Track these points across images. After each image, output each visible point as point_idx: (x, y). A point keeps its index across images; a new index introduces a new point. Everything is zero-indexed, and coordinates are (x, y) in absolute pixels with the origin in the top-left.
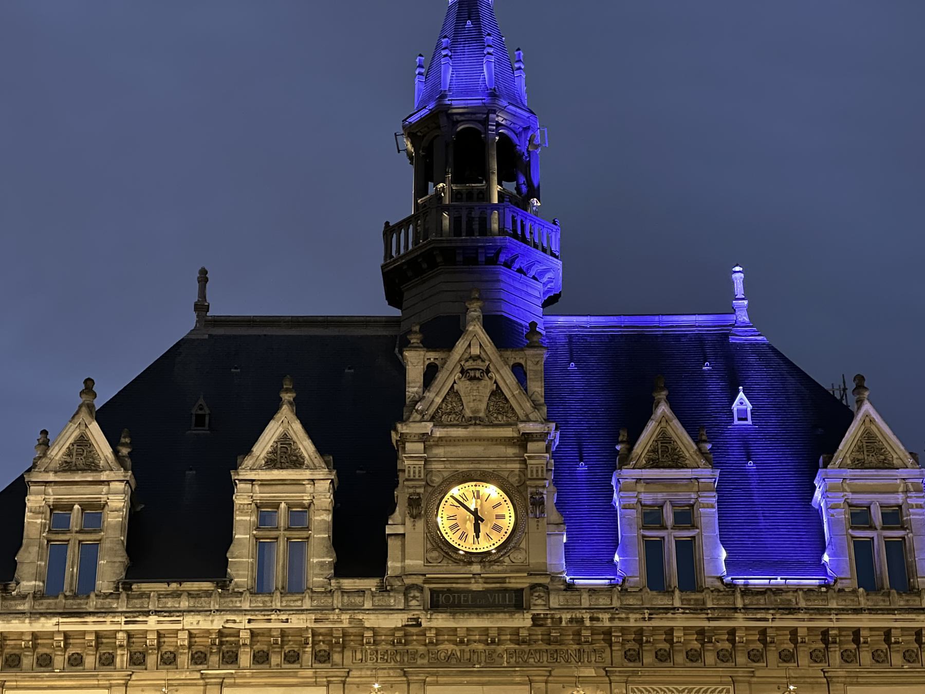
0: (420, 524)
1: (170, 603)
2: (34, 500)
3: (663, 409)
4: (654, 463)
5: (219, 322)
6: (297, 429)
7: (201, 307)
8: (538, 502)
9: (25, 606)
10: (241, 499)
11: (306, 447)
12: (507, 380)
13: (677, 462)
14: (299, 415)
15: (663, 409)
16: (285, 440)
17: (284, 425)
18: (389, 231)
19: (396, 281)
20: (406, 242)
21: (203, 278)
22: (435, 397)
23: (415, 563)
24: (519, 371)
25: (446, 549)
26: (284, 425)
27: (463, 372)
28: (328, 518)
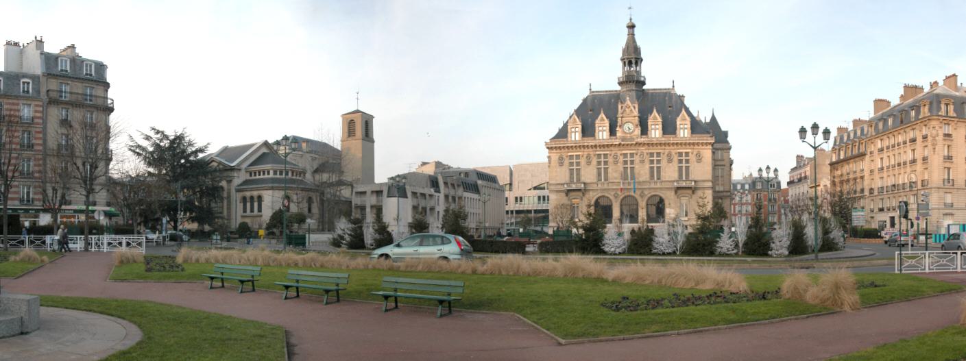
2: (569, 127)
3: (655, 111)
5: (593, 92)
6: (604, 116)
7: (590, 90)
10: (597, 125)
11: (605, 118)
12: (632, 108)
14: (604, 114)
15: (655, 111)
17: (602, 115)
18: (618, 78)
19: (620, 83)
21: (590, 85)
24: (634, 107)
25: (625, 133)
26: (602, 115)
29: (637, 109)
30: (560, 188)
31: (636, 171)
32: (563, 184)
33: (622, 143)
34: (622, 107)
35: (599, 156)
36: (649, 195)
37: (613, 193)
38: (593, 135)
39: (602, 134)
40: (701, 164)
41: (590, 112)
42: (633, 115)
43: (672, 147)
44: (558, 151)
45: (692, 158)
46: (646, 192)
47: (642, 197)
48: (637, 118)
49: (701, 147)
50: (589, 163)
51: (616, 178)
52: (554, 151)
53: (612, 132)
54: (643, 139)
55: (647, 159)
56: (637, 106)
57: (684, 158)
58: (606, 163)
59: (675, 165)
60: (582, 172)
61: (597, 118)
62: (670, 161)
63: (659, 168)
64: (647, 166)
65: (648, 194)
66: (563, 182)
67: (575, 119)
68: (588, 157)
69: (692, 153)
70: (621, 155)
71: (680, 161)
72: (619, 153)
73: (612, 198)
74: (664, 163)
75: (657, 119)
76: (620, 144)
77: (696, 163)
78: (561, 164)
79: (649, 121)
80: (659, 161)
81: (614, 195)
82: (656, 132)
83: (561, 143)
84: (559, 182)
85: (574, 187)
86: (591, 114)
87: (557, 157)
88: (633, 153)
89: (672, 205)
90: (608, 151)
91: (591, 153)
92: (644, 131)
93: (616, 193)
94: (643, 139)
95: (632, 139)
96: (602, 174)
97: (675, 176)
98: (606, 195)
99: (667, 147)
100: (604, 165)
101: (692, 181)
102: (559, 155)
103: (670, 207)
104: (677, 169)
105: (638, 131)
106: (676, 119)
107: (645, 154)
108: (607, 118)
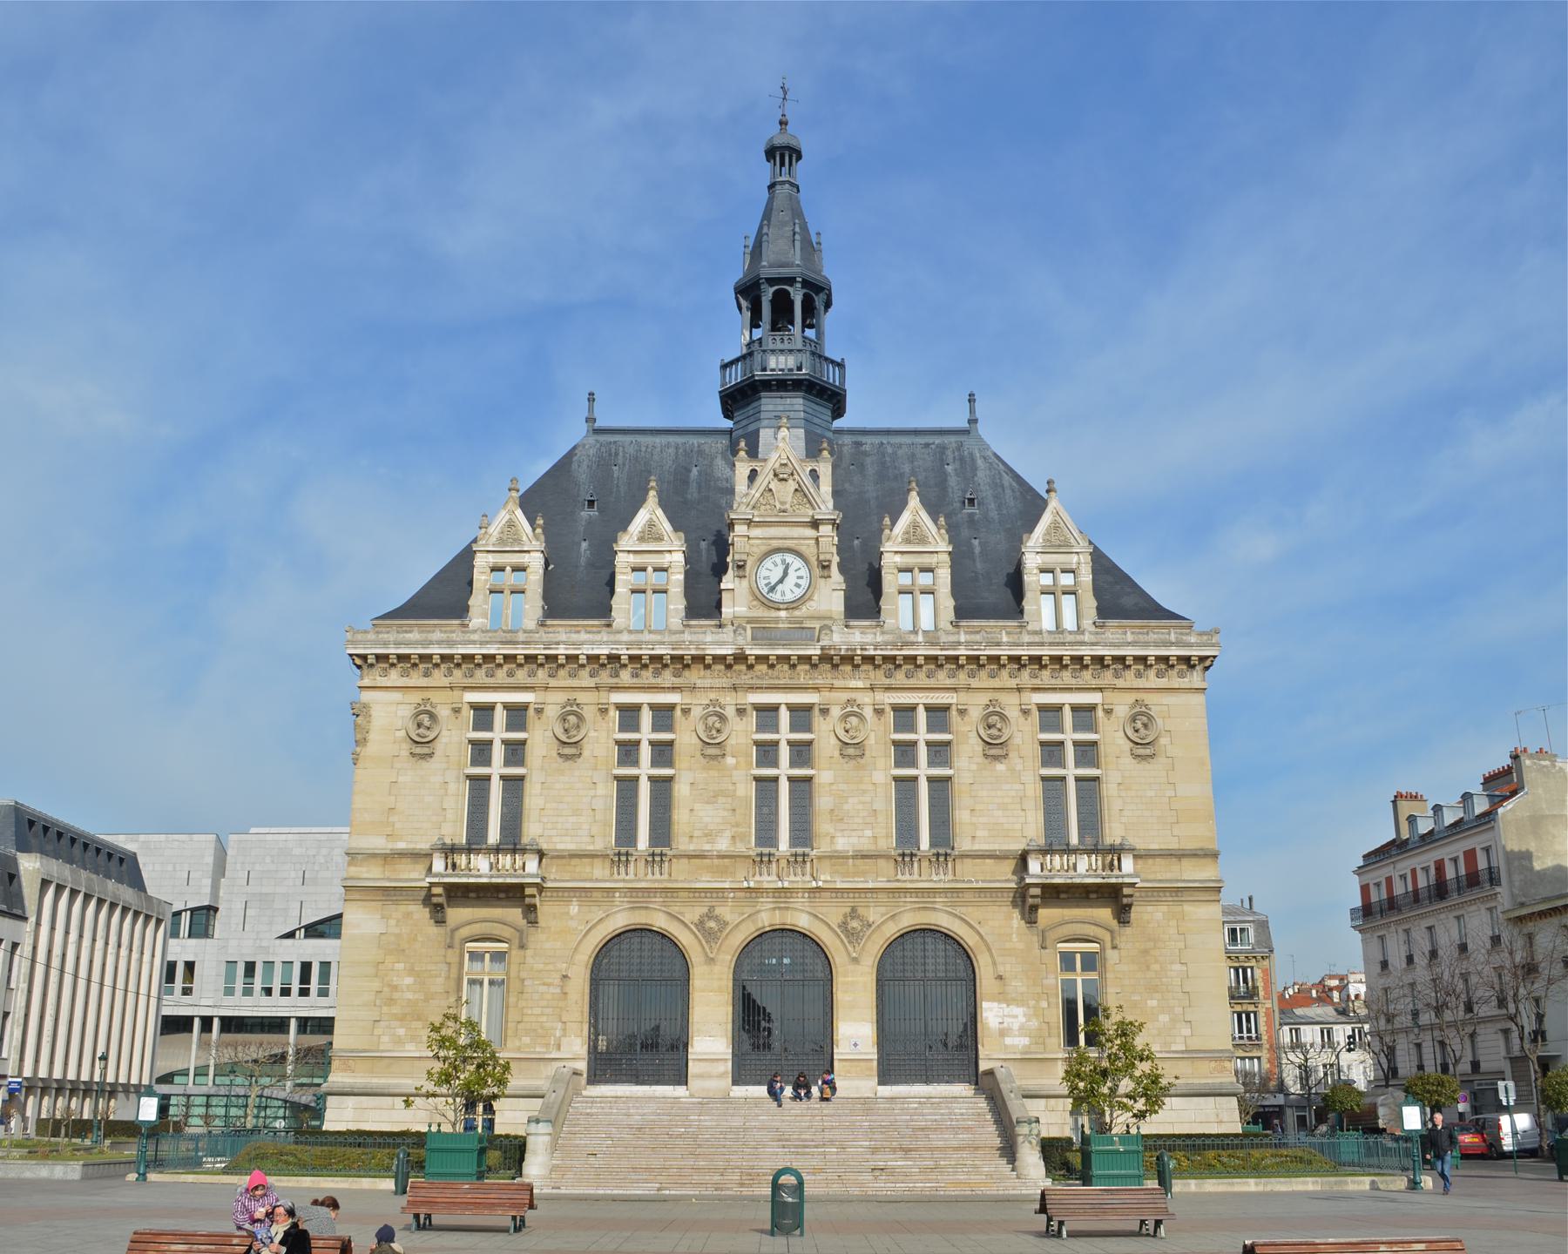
0: (745, 582)
1: (574, 637)
2: (481, 562)
3: (914, 501)
4: (908, 541)
8: (825, 567)
9: (475, 637)
10: (622, 561)
11: (666, 526)
13: (923, 540)
14: (663, 504)
15: (914, 501)
16: (651, 524)
20: (736, 376)
22: (756, 492)
23: (741, 610)
26: (650, 513)
27: (776, 475)
28: (681, 577)
29: (826, 487)
30: (414, 875)
31: (823, 802)
32: (415, 856)
33: (753, 651)
34: (753, 475)
35: (629, 715)
36: (892, 930)
37: (692, 914)
38: (599, 607)
39: (646, 609)
40: (1156, 768)
41: (586, 514)
42: (807, 514)
43: (1005, 679)
44: (416, 679)
45: (1112, 736)
46: (873, 914)
47: (852, 936)
48: (826, 530)
49: (1151, 679)
50: (569, 748)
51: (710, 835)
52: (394, 677)
53: (703, 601)
54: (860, 637)
55: (878, 735)
56: (825, 469)
57: (1069, 736)
58: (663, 752)
59: (1026, 770)
60: (533, 798)
61: (624, 524)
62: (995, 748)
63: (940, 785)
64: (882, 771)
65: (887, 922)
66: (423, 845)
67: (511, 524)
68: (572, 715)
69: (1108, 712)
70: (741, 712)
71: (1051, 752)
72: (729, 701)
73: (685, 938)
74: (967, 763)
75: (923, 540)
76: (740, 658)
77: (1128, 761)
78: (422, 746)
79: (887, 547)
80: (940, 752)
81: (700, 924)
82: (919, 609)
83: (434, 637)
84: (401, 845)
85: (481, 868)
86: (590, 522)
87: (406, 712)
88: (808, 708)
89: (1017, 985)
90: (673, 689)
91: (582, 697)
92: (866, 596)
93: (710, 915)
94: (860, 637)
95: (801, 632)
96: (644, 816)
97: (1030, 827)
98: (660, 922)
99: (982, 679)
100: (655, 763)
101: (1117, 851)
102: (416, 697)
103: (1002, 997)
104: (1035, 790)
105: (831, 597)
106: (1019, 542)
107: (868, 712)
108: (676, 529)
